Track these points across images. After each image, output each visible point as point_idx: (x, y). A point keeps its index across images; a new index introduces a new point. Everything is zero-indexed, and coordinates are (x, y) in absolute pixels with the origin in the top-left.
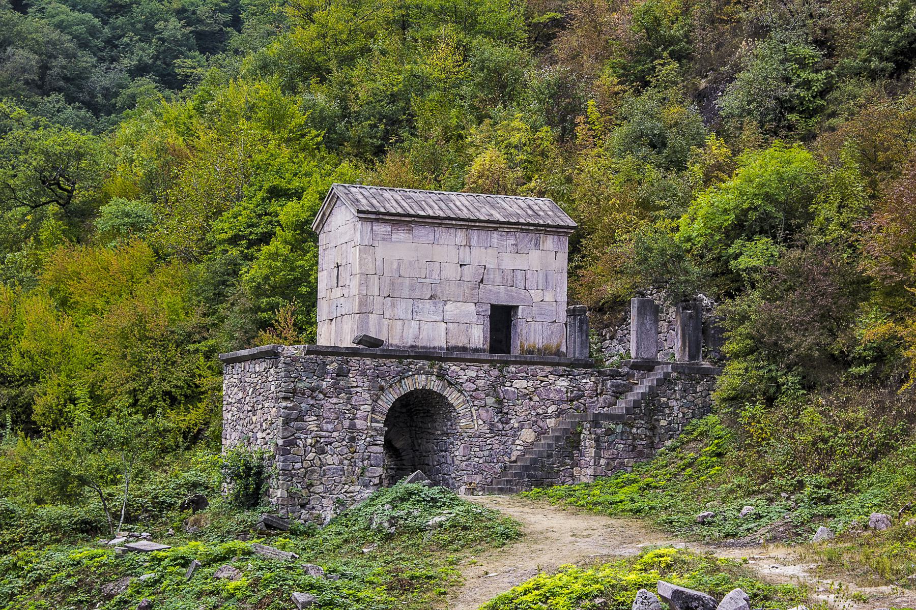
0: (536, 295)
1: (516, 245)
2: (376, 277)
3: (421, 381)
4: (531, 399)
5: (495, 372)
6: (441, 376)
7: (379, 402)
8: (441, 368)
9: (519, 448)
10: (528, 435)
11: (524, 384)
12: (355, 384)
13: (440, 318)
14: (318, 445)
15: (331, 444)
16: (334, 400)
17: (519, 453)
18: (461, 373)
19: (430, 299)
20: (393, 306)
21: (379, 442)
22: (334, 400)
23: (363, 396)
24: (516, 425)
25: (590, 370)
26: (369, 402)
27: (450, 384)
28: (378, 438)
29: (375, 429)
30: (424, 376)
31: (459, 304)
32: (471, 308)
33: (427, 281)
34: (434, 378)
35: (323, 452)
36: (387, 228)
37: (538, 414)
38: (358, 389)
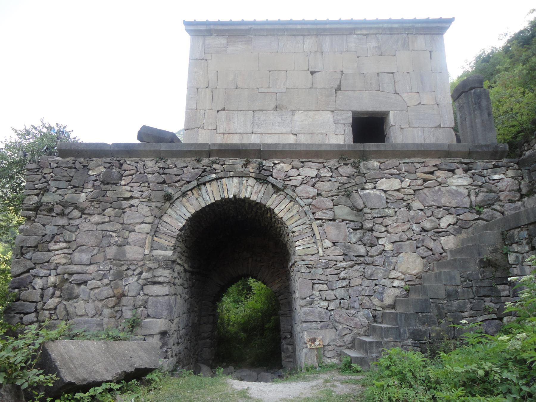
0: (410, 99)
1: (379, 47)
2: (208, 91)
3: (232, 188)
4: (409, 207)
5: (347, 170)
6: (262, 179)
7: (166, 218)
8: (261, 167)
9: (396, 283)
10: (411, 264)
11: (395, 183)
12: (128, 195)
13: (289, 130)
14: (66, 285)
15: (85, 283)
16: (96, 218)
17: (397, 292)
18: (293, 172)
19: (276, 108)
20: (229, 119)
21: (161, 279)
22: (96, 218)
23: (139, 214)
24: (389, 247)
25: (504, 161)
26: (149, 219)
27: (277, 190)
28: (161, 272)
29: (156, 260)
30: (236, 180)
31: (311, 113)
32: (327, 116)
33: (271, 90)
34: (251, 181)
35: (71, 297)
36: (222, 41)
37: (424, 230)
38: (132, 202)
